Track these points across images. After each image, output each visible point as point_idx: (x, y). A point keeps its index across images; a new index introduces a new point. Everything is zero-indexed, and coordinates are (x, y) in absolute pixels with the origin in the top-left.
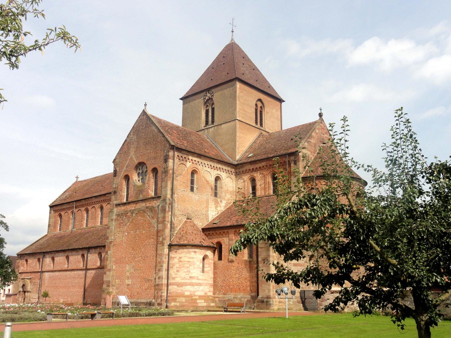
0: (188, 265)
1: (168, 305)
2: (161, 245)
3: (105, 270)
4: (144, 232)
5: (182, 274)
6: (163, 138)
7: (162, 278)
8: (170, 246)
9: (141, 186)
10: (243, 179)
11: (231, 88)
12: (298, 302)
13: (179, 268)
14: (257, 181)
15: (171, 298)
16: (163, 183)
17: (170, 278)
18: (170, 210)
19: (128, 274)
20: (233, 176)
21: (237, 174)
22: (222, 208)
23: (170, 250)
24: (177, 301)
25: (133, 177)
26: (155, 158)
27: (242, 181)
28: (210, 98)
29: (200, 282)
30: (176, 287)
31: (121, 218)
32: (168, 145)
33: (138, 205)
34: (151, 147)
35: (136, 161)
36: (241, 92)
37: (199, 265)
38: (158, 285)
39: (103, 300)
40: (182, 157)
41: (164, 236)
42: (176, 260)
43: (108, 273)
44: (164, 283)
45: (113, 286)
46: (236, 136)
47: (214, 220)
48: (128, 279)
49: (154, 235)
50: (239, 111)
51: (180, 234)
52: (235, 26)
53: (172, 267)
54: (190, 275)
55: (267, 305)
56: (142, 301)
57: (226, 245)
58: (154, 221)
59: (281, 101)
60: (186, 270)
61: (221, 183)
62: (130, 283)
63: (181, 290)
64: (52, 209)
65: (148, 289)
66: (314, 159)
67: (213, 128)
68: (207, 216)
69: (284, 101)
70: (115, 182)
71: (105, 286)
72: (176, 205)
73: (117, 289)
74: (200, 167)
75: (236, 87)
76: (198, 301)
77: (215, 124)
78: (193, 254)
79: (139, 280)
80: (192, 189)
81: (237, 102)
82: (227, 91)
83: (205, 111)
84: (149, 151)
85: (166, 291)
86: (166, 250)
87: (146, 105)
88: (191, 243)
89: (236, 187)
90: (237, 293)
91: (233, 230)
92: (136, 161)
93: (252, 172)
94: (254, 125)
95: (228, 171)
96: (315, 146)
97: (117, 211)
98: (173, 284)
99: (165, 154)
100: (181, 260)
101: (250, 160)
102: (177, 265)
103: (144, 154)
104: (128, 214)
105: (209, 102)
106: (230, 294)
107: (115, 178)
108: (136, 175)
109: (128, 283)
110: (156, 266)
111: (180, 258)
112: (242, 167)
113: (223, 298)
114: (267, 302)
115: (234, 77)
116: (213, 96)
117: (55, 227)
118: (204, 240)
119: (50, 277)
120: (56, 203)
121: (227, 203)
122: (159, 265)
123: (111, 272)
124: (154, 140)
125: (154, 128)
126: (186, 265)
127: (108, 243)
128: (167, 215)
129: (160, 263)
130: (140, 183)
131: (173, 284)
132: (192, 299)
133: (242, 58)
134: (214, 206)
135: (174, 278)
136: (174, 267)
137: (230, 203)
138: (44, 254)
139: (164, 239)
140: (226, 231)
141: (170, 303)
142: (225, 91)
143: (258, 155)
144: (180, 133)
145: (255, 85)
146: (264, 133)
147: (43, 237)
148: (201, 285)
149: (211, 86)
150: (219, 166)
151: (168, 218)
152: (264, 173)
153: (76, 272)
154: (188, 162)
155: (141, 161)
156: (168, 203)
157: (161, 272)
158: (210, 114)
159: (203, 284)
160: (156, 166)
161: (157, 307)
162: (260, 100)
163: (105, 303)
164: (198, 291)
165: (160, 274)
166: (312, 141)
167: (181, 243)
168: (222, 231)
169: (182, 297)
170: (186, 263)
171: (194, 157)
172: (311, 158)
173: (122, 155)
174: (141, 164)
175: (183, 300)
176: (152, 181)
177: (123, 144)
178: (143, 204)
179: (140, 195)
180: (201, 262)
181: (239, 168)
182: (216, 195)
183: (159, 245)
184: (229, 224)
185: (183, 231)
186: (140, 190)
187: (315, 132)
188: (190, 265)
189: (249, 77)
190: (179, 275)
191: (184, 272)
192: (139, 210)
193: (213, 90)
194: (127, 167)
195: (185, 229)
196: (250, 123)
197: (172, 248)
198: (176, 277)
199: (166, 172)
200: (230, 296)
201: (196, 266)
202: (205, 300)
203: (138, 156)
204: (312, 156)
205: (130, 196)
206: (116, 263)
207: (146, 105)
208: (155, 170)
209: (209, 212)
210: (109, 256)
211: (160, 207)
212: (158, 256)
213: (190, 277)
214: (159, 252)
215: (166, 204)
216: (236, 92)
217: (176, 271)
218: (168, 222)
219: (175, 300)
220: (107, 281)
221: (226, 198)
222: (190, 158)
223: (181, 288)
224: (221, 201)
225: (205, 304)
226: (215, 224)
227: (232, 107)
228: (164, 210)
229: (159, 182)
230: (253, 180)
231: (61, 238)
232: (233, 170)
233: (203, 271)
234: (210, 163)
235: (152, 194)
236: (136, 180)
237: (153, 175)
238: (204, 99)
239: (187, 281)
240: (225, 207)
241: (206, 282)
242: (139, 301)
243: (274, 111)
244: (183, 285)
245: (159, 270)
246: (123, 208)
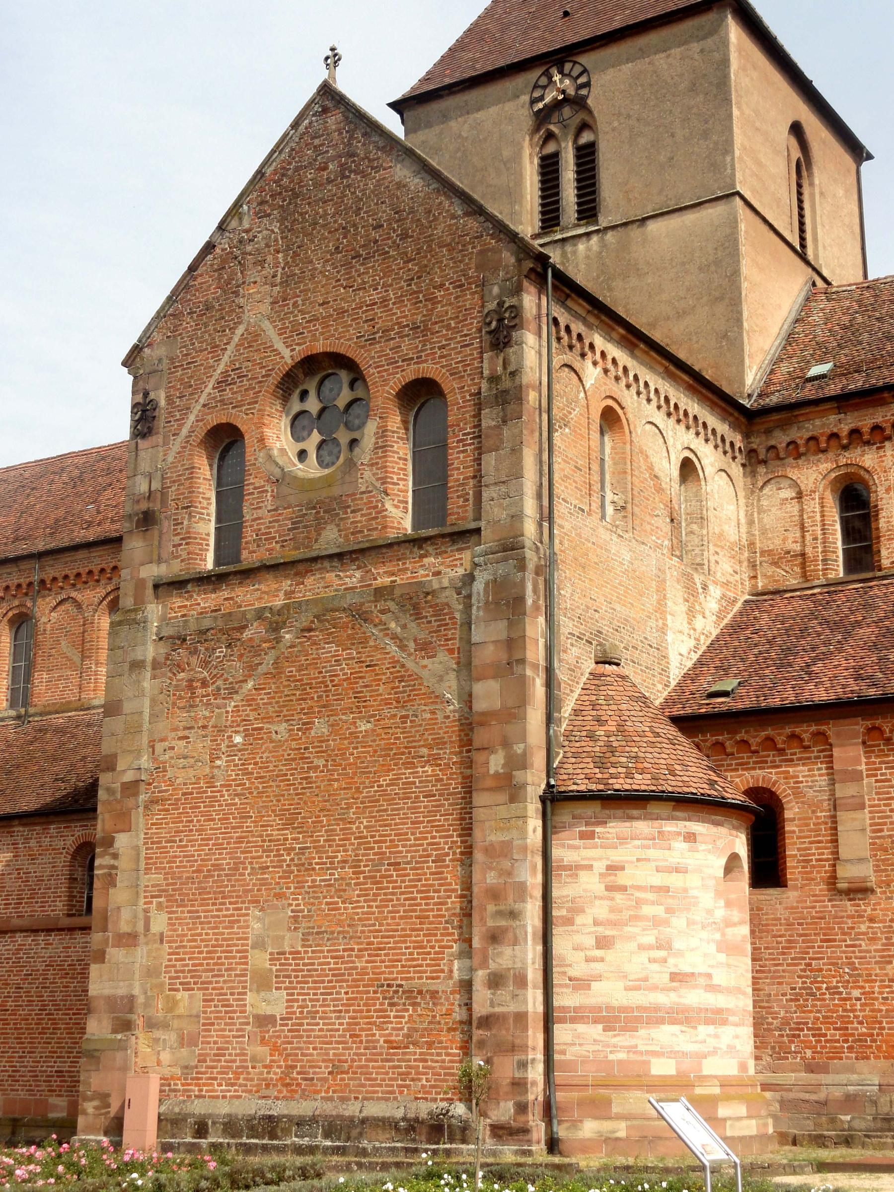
0: (659, 911)
1: (561, 1132)
2: (503, 797)
3: (96, 937)
4: (363, 727)
5: (631, 957)
6: (473, 224)
7: (521, 981)
8: (553, 800)
9: (327, 482)
10: (795, 484)
11: (695, 47)
14: (881, 490)
15: (575, 1095)
16: (490, 461)
17: (557, 980)
18: (541, 602)
19: (260, 960)
20: (736, 470)
21: (753, 460)
24: (615, 1109)
25: (268, 432)
26: (420, 330)
27: (788, 493)
28: (566, 100)
30: (595, 1031)
31: (195, 652)
32: (508, 257)
33: (309, 580)
34: (387, 272)
35: (286, 353)
36: (744, 69)
37: (709, 912)
38: (487, 1021)
39: (90, 1107)
40: (568, 329)
41: (519, 748)
42: (590, 883)
43: (115, 954)
44: (530, 1008)
45: (151, 1025)
46: (736, 272)
47: (692, 676)
48: (263, 983)
49: (440, 743)
50: (741, 158)
51: (591, 736)
53: (569, 921)
56: (375, 1110)
57: (815, 806)
58: (438, 671)
59: (857, 151)
60: (649, 939)
61: (697, 494)
63: (632, 1049)
65: (411, 1040)
67: (595, 239)
69: (870, 157)
70: (145, 465)
71: (97, 1028)
72: (558, 576)
73: (187, 1040)
74: (629, 398)
75: (725, 43)
77: (604, 221)
78: (680, 845)
79: (343, 992)
81: (736, 112)
82: (668, 60)
83: (536, 161)
85: (540, 1056)
86: (534, 824)
87: (333, 59)
88: (670, 785)
89: (751, 523)
91: (860, 726)
92: (286, 353)
93: (845, 448)
95: (723, 440)
97: (163, 619)
98: (578, 1016)
99: (492, 306)
100: (622, 879)
101: (833, 389)
103: (342, 312)
104: (247, 634)
106: (852, 1070)
107: (143, 444)
108: (284, 423)
109: (265, 1009)
110: (467, 914)
111: (613, 868)
112: (784, 425)
113: (808, 1088)
116: (587, 85)
122: (491, 908)
123: (141, 955)
124: (404, 236)
125: (402, 172)
126: (647, 910)
127: (109, 790)
128: (530, 632)
129: (495, 895)
130: (311, 470)
131: (578, 1016)
134: (682, 608)
135: (581, 984)
136: (579, 920)
139: (521, 763)
140: (806, 731)
141: (575, 1124)
142: (660, 60)
143: (872, 364)
146: (820, 283)
148: (724, 1022)
149: (572, 38)
150: (694, 407)
151: (536, 653)
154: (588, 363)
156: (531, 566)
157: (508, 951)
160: (430, 369)
161: (490, 1144)
162: (796, 129)
163: (103, 1122)
164: (714, 1052)
165: (504, 958)
167: (620, 784)
168: (780, 735)
169: (640, 1087)
170: (650, 896)
171: (610, 340)
173: (188, 323)
174: (319, 366)
176: (401, 451)
177: (192, 268)
179: (319, 530)
181: (768, 432)
183: (480, 799)
185: (599, 721)
186: (323, 505)
190: (605, 965)
191: (641, 947)
192: (324, 613)
193: (585, 60)
194: (222, 384)
197: (565, 814)
198: (598, 978)
199: (505, 395)
200: (854, 1077)
201: (699, 916)
202: (749, 1101)
203: (295, 326)
205: (249, 535)
206: (171, 897)
207: (333, 59)
208: (420, 394)
209: (670, 637)
210: (124, 863)
211: (479, 586)
212: (478, 856)
213: (676, 977)
214: (487, 834)
215: (522, 566)
216: (725, 62)
217: (590, 941)
218: (535, 667)
219: (599, 1108)
220: (112, 1002)
222: (599, 341)
223: (623, 1040)
224: (705, 587)
226: (725, 694)
227: (705, 135)
228: (509, 604)
229: (459, 461)
232: (738, 440)
234: (667, 388)
235: (401, 519)
236: (283, 451)
237: (405, 422)
238: (533, 102)
239: (662, 999)
242: (352, 1109)
243: (841, 192)
244: (639, 1020)
245: (494, 937)
246: (205, 601)
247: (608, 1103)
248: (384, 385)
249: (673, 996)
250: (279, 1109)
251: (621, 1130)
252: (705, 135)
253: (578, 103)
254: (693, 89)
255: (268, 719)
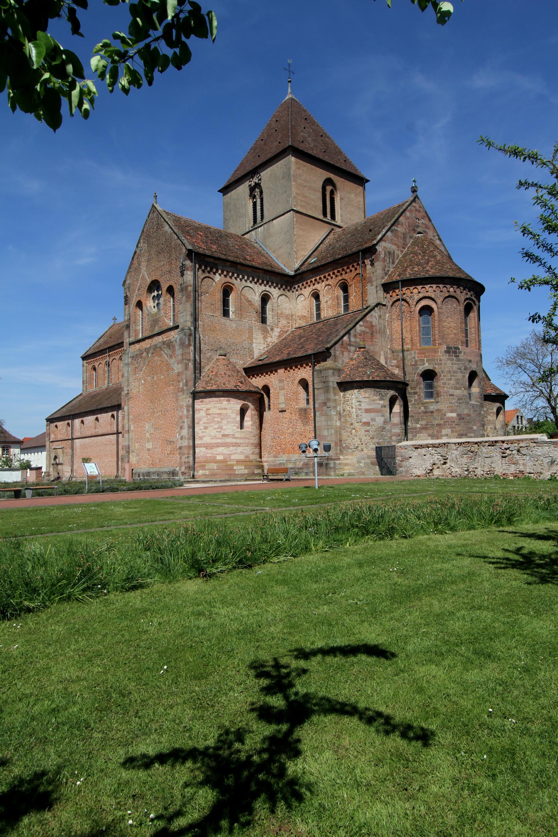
0: (219, 419)
6: (179, 241)
9: (156, 314)
12: (372, 463)
13: (207, 423)
18: (192, 343)
19: (148, 435)
22: (274, 338)
23: (194, 399)
25: (147, 302)
26: (170, 272)
29: (238, 441)
36: (299, 168)
42: (203, 413)
47: (261, 356)
48: (148, 442)
49: (173, 380)
51: (208, 376)
52: (294, 73)
53: (198, 423)
54: (223, 432)
55: (327, 468)
60: (216, 426)
62: (150, 447)
63: (212, 453)
64: (85, 362)
66: (403, 257)
68: (251, 351)
69: (368, 181)
76: (235, 468)
77: (264, 221)
78: (225, 403)
80: (226, 313)
81: (293, 183)
84: (162, 263)
90: (291, 455)
94: (321, 217)
96: (404, 238)
100: (210, 412)
102: (205, 420)
105: (256, 191)
114: (327, 464)
115: (287, 145)
117: (91, 383)
118: (241, 383)
119: (81, 446)
120: (89, 353)
121: (282, 332)
126: (216, 419)
130: (155, 310)
131: (201, 446)
132: (227, 466)
133: (303, 121)
135: (201, 438)
137: (286, 332)
138: (73, 417)
141: (198, 471)
144: (209, 235)
145: (321, 158)
147: (77, 397)
148: (239, 446)
152: (330, 283)
153: (107, 437)
155: (154, 278)
158: (258, 208)
159: (242, 443)
160: (172, 283)
166: (399, 229)
172: (398, 255)
175: (214, 466)
178: (159, 339)
180: (237, 414)
182: (264, 320)
184: (277, 359)
186: (155, 321)
187: (405, 216)
188: (222, 419)
189: (312, 145)
190: (206, 434)
191: (214, 429)
195: (215, 370)
196: (314, 215)
198: (204, 436)
204: (400, 253)
209: (254, 345)
213: (223, 435)
217: (202, 428)
219: (203, 467)
221: (280, 325)
223: (210, 451)
224: (272, 329)
225: (246, 471)
227: (285, 192)
230: (316, 296)
231: (93, 396)
233: (242, 427)
236: (150, 307)
239: (219, 441)
240: (279, 336)
241: (247, 441)
246: (137, 346)
247: (205, 466)
248: (164, 287)
249: (223, 440)
250: (151, 470)
251: (207, 472)
252: (285, 192)
253: (258, 185)
254: (283, 178)
255: (147, 376)
